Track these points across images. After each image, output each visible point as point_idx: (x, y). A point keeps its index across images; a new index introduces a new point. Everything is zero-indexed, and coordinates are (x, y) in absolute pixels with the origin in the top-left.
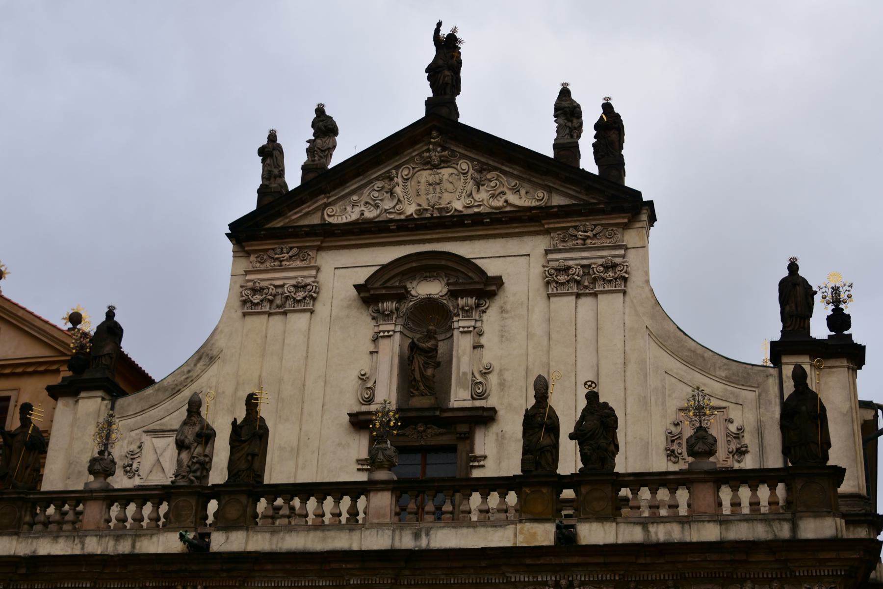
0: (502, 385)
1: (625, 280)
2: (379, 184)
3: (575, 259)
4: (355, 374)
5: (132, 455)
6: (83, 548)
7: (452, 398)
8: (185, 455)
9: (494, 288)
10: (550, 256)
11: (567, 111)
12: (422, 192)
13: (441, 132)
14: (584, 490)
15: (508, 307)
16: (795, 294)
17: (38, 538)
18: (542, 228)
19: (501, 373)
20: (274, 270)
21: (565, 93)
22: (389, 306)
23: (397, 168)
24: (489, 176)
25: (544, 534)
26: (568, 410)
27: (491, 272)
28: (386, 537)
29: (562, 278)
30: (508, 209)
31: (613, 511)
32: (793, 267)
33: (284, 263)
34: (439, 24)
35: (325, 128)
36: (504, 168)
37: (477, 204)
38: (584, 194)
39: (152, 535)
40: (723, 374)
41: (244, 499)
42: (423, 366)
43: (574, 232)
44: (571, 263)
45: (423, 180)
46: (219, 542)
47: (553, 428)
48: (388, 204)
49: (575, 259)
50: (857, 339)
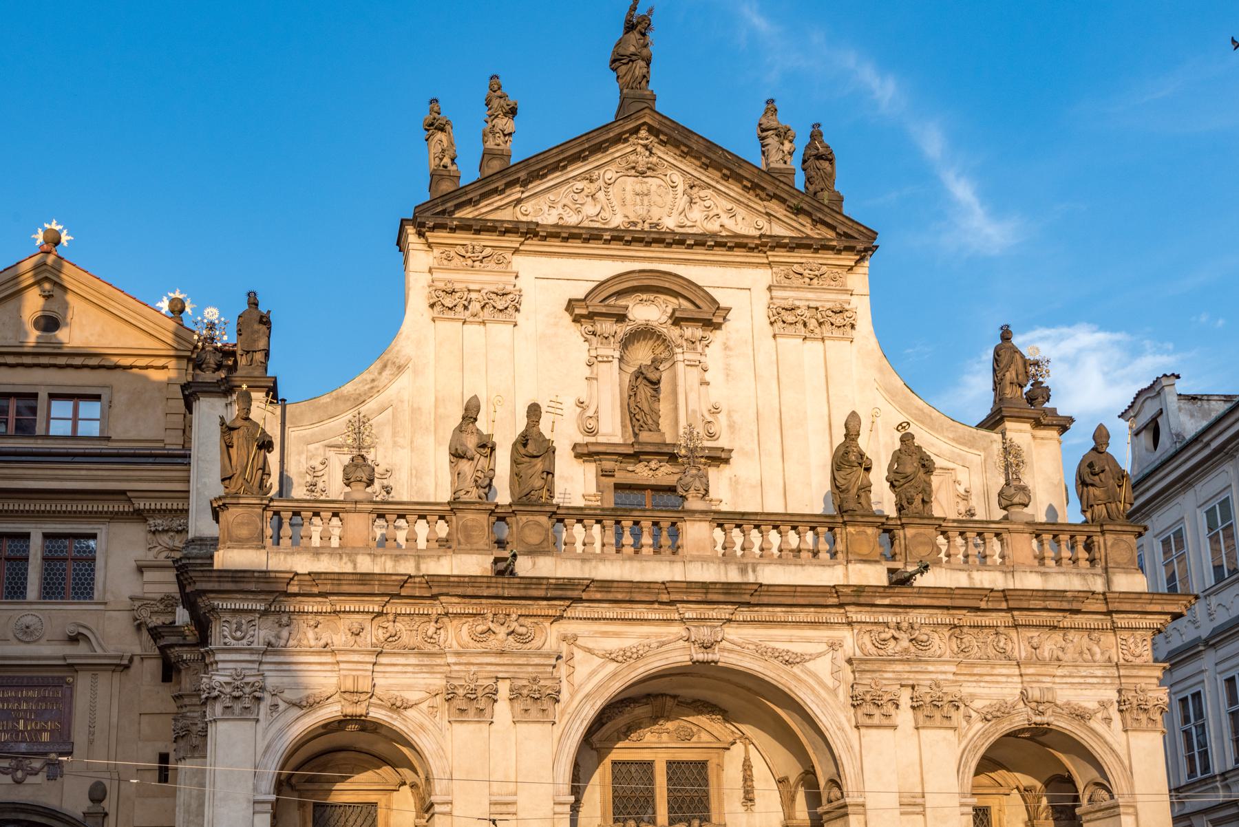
1: (853, 326)
2: (580, 185)
3: (801, 297)
6: (355, 567)
9: (721, 320)
12: (628, 201)
17: (293, 554)
18: (766, 261)
23: (597, 167)
24: (702, 193)
25: (875, 575)
28: (712, 570)
29: (790, 318)
30: (724, 234)
33: (477, 264)
36: (718, 186)
37: (689, 224)
39: (439, 557)
41: (544, 519)
43: (801, 271)
44: (797, 303)
45: (629, 188)
46: (524, 566)
48: (590, 209)
49: (801, 297)
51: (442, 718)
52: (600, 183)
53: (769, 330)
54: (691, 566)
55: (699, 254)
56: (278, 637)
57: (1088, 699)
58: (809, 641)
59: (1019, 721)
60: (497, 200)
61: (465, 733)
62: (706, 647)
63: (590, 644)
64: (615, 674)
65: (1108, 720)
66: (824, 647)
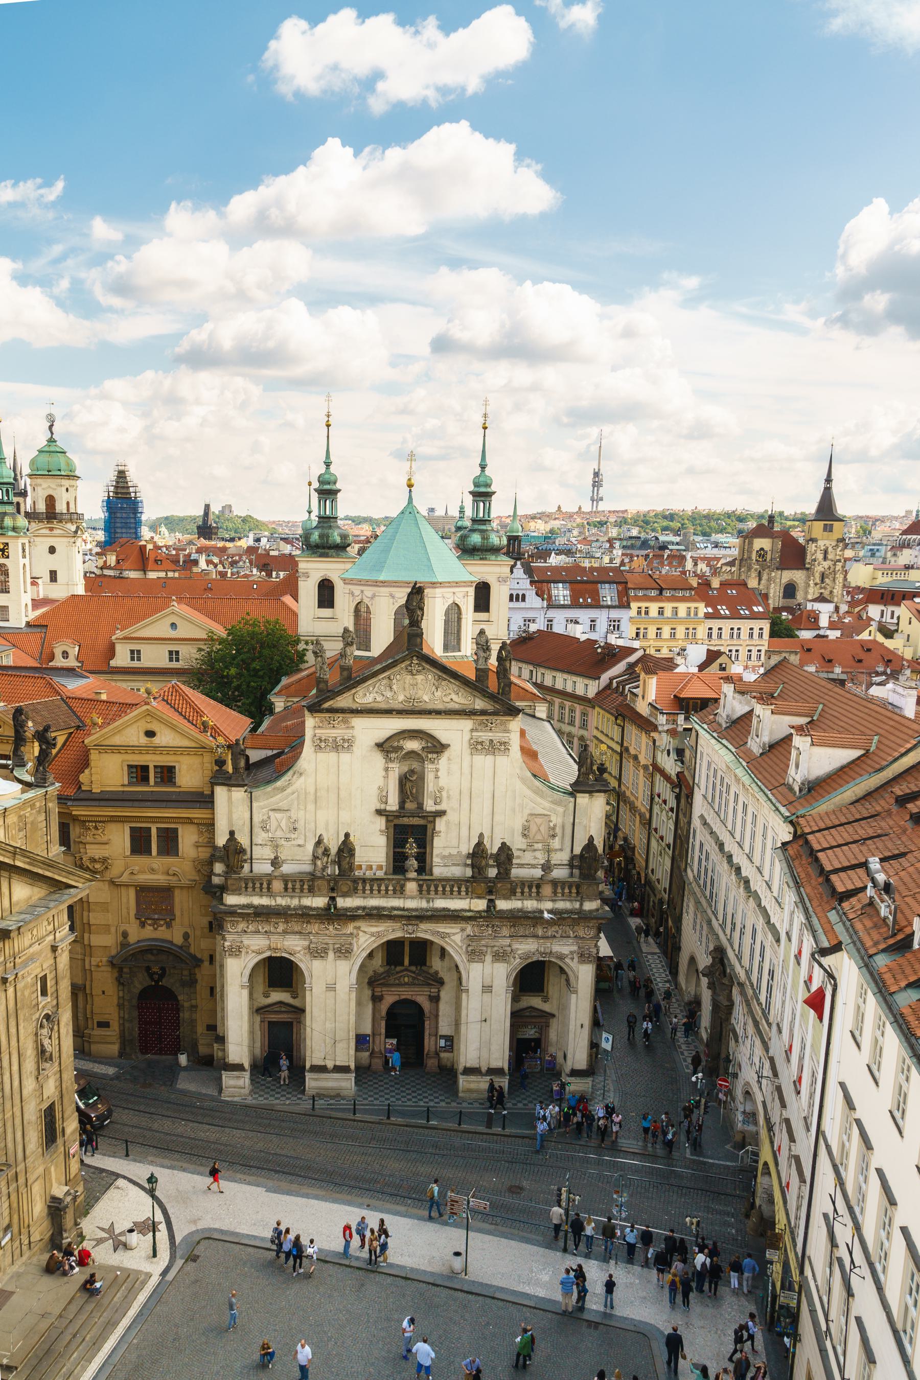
0: (448, 797)
2: (384, 682)
3: (485, 736)
4: (377, 787)
5: (263, 821)
8: (319, 863)
10: (474, 734)
15: (451, 757)
19: (448, 792)
20: (330, 728)
22: (393, 755)
24: (444, 683)
29: (479, 747)
31: (511, 894)
41: (349, 883)
42: (410, 786)
46: (342, 903)
51: (308, 956)
52: (394, 681)
53: (469, 751)
56: (248, 927)
57: (565, 950)
58: (452, 928)
59: (535, 959)
60: (345, 695)
61: (317, 964)
64: (374, 941)
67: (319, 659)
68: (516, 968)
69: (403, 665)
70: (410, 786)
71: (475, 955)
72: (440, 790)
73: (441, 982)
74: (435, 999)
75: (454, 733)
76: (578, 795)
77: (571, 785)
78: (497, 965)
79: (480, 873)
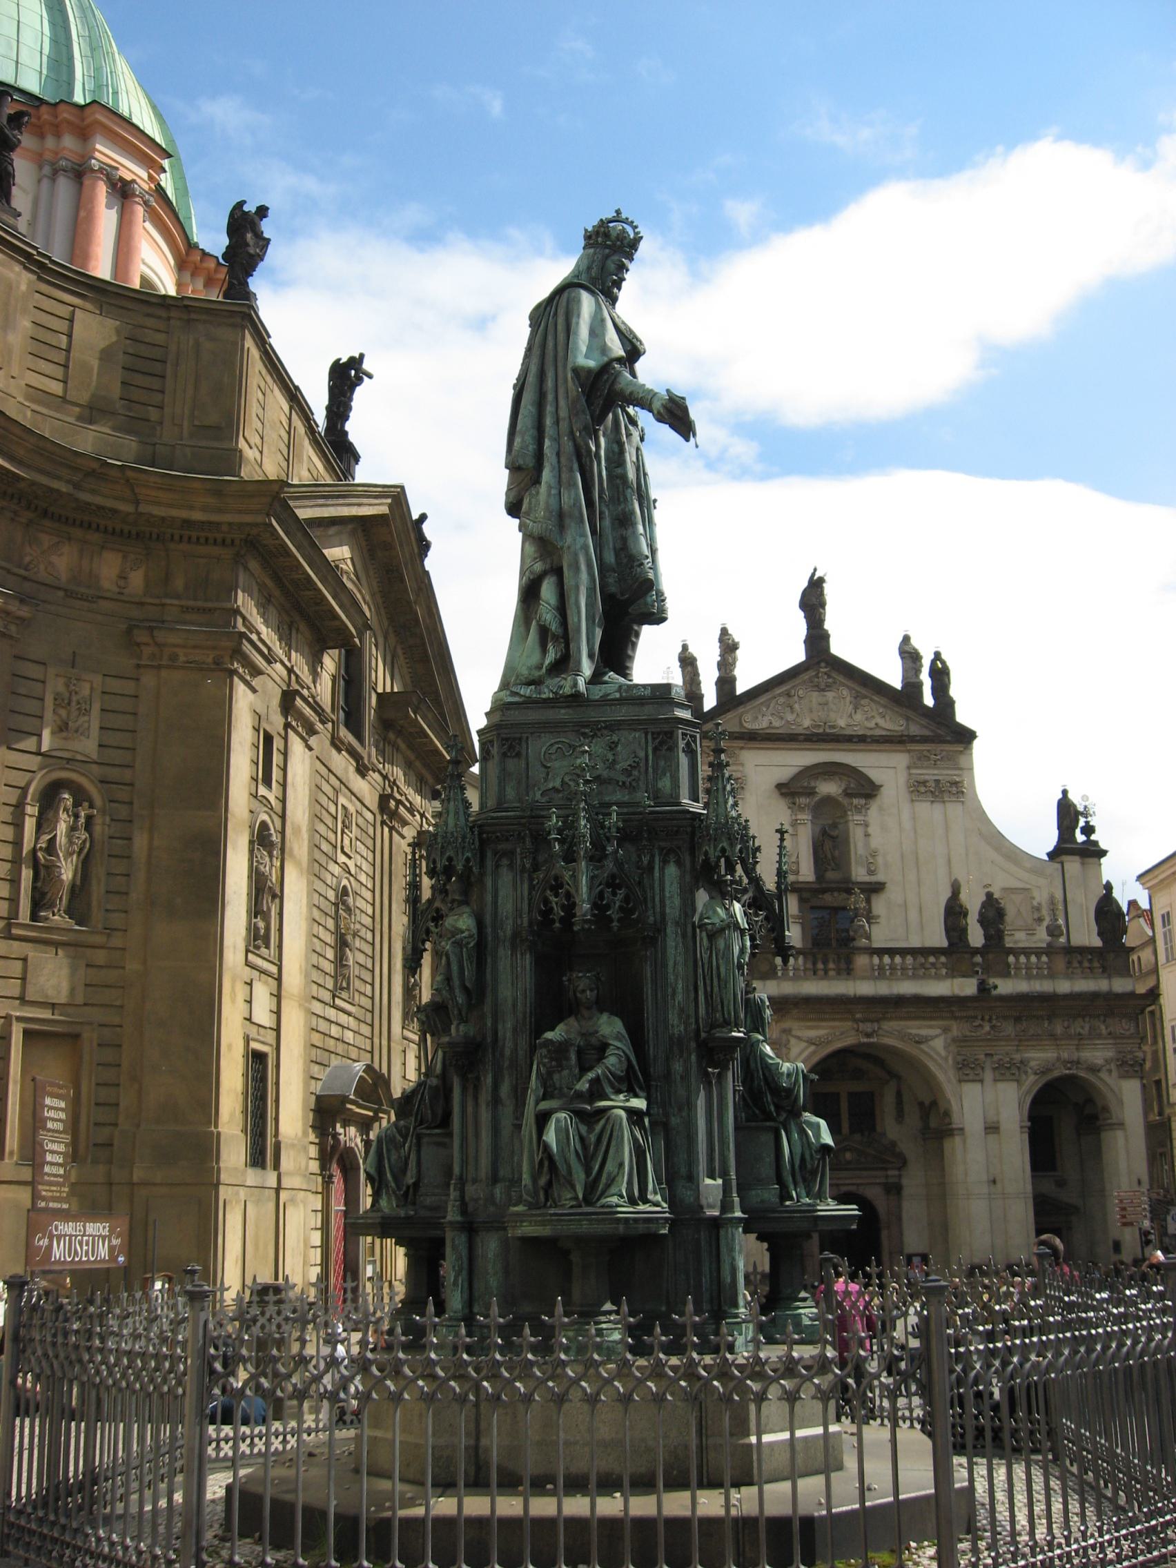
2: (782, 700)
3: (930, 774)
7: (853, 874)
11: (909, 655)
13: (828, 664)
14: (991, 956)
16: (1067, 813)
21: (906, 639)
22: (803, 800)
24: (863, 702)
26: (972, 901)
27: (877, 783)
29: (922, 789)
32: (1065, 792)
34: (815, 570)
35: (728, 647)
38: (926, 722)
40: (1028, 865)
41: (770, 956)
42: (830, 847)
44: (927, 777)
47: (966, 915)
48: (790, 717)
49: (930, 774)
50: (1103, 846)
54: (858, 982)
55: (861, 746)
58: (931, 1027)
59: (1056, 1074)
60: (729, 715)
62: (868, 1035)
63: (799, 1033)
64: (814, 1053)
65: (1110, 1071)
66: (938, 1031)
67: (689, 668)
68: (1028, 1092)
69: (805, 676)
70: (830, 847)
71: (968, 1070)
72: (874, 854)
73: (903, 1162)
74: (894, 1190)
75: (888, 770)
76: (1065, 858)
77: (1048, 854)
78: (1001, 1085)
79: (961, 940)
